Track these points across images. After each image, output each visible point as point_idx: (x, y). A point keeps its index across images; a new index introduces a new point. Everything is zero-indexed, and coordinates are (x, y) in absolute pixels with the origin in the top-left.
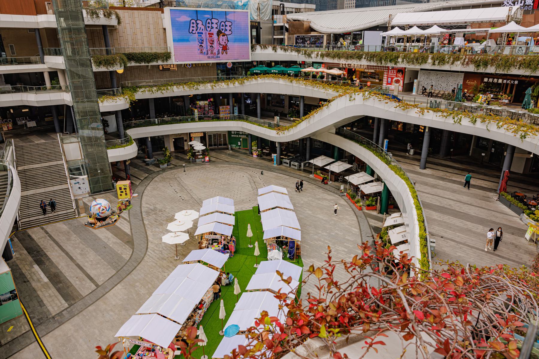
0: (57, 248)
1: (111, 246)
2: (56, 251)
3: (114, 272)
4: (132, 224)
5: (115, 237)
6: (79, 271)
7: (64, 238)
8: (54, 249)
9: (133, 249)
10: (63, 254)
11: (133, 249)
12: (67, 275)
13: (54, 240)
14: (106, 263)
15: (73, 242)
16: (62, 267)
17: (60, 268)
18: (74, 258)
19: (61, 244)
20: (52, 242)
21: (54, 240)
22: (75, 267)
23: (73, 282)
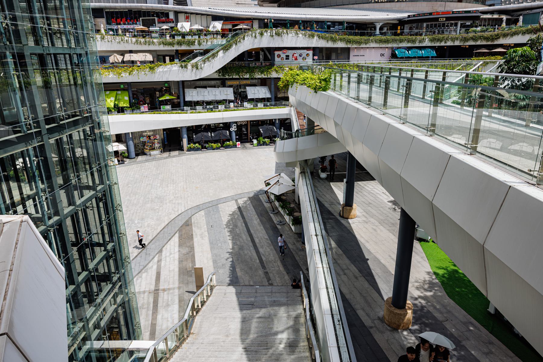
0: (257, 241)
1: (206, 226)
2: (258, 238)
3: (219, 205)
4: (162, 246)
5: (194, 234)
6: (244, 213)
7: (246, 252)
8: (260, 241)
9: (191, 217)
10: (252, 232)
11: (191, 217)
12: (254, 213)
13: (258, 252)
14: (221, 213)
15: (238, 243)
16: (256, 220)
17: (258, 220)
18: (244, 225)
19: (251, 244)
20: (261, 250)
21: (258, 252)
22: (246, 217)
23: (252, 207)
